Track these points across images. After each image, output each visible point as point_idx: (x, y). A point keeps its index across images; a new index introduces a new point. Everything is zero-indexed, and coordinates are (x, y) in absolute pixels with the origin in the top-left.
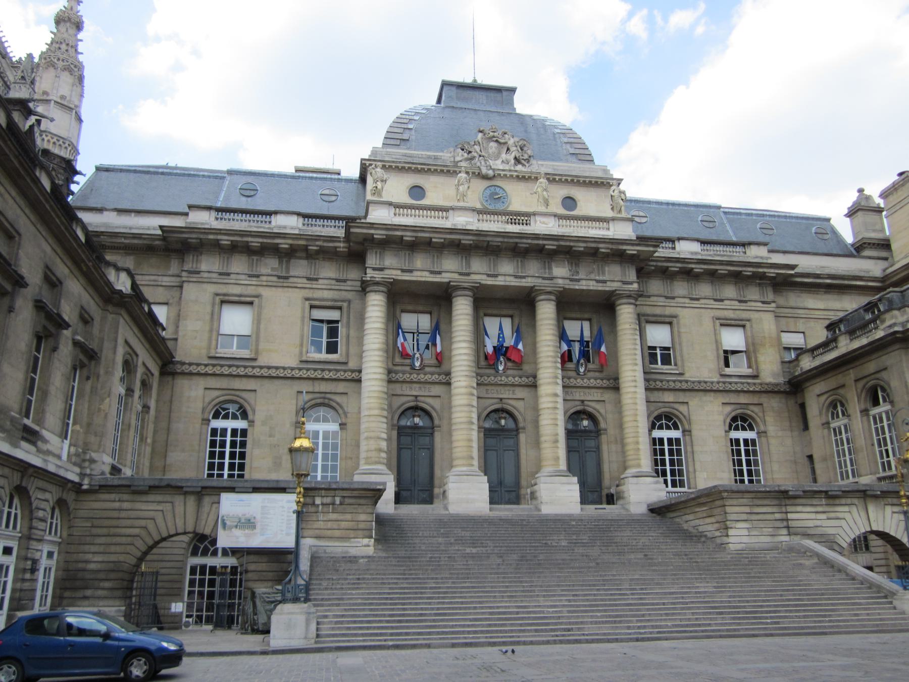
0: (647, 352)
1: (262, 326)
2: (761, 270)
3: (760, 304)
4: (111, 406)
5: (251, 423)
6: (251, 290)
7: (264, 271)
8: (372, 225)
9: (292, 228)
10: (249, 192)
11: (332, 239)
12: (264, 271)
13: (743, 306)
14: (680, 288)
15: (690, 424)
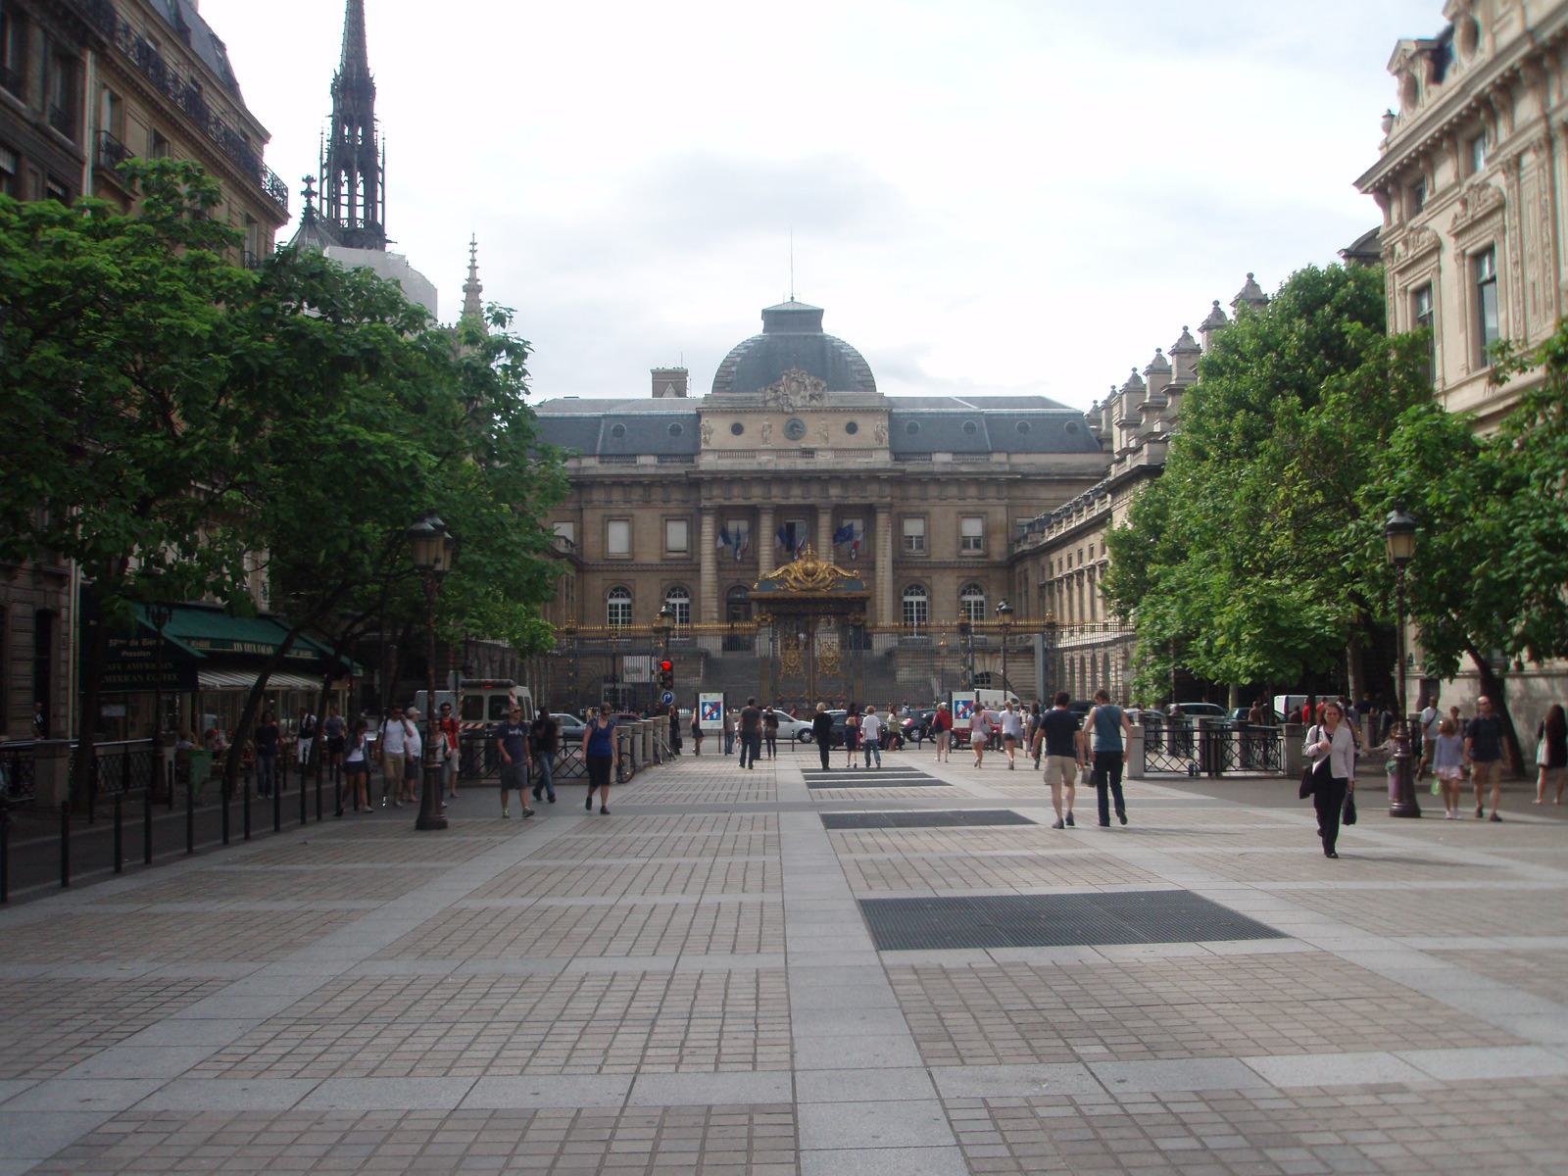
4: (563, 612)
5: (634, 601)
8: (702, 472)
10: (619, 432)
11: (678, 475)
14: (933, 491)
15: (931, 590)
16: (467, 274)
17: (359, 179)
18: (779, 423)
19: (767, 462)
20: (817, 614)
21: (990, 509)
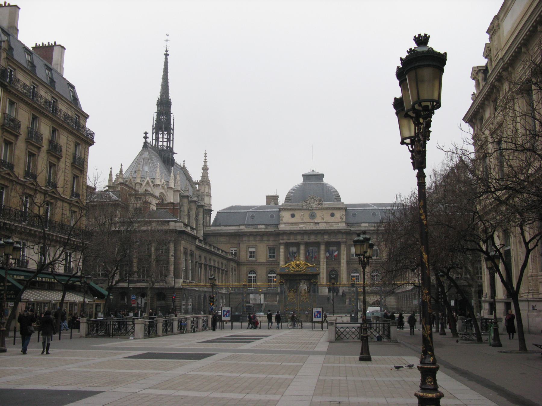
10: (253, 217)
12: (257, 239)
16: (203, 164)
17: (165, 133)
18: (307, 214)
19: (302, 227)
20: (300, 280)
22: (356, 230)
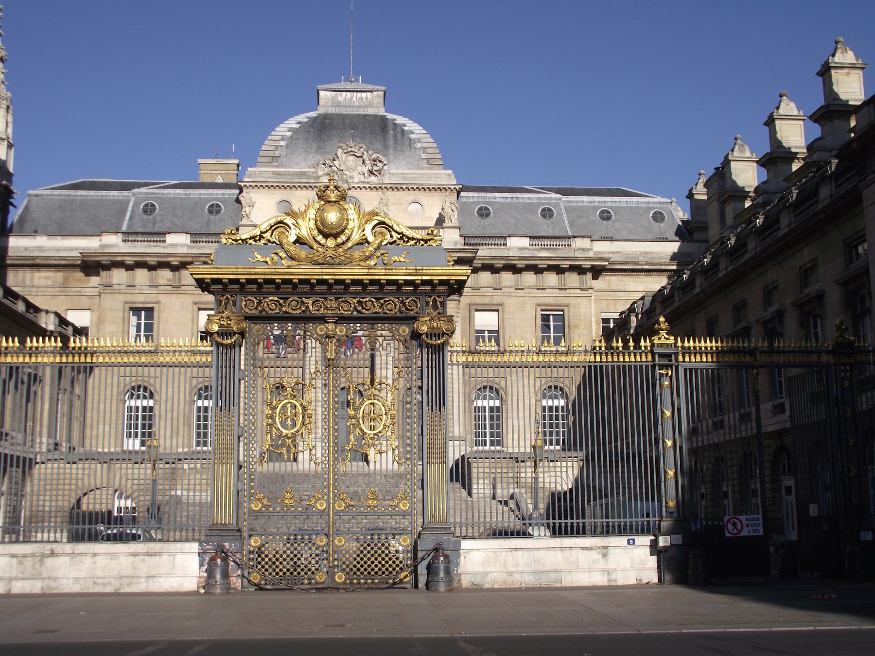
0: (474, 335)
1: (161, 326)
2: (577, 263)
3: (579, 291)
6: (152, 298)
7: (161, 281)
9: (183, 245)
13: (563, 293)
21: (572, 301)
22: (494, 258)
